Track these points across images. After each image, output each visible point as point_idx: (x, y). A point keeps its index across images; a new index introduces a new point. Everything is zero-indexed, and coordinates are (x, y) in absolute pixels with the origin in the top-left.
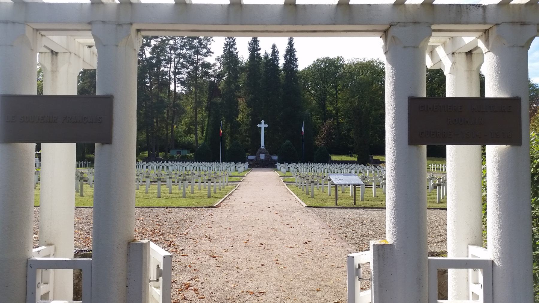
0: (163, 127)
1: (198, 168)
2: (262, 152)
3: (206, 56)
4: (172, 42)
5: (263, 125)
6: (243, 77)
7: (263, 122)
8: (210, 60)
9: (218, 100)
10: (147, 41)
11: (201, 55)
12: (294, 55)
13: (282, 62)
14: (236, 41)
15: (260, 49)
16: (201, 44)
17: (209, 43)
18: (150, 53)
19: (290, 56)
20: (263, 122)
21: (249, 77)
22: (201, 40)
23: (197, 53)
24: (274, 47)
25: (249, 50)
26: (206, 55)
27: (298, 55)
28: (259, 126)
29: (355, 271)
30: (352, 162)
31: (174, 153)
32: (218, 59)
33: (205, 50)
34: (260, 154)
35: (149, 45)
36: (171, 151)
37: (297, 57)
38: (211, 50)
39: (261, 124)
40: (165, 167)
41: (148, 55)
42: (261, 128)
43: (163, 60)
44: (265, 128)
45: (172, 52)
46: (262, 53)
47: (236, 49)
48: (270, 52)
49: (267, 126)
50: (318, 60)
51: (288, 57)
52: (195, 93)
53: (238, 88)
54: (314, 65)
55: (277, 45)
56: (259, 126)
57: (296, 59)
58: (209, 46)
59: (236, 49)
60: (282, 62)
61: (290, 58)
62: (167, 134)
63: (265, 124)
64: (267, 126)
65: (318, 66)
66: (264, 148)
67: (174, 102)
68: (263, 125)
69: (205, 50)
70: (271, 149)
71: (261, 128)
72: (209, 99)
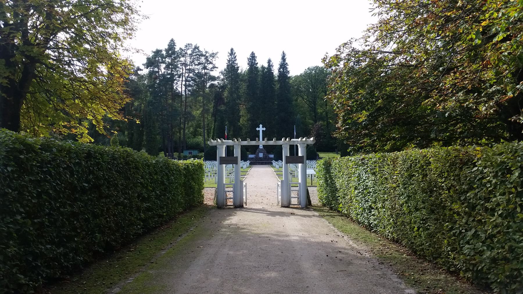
0: (177, 132)
3: (212, 71)
4: (182, 59)
6: (243, 87)
7: (261, 126)
8: (215, 73)
9: (223, 108)
10: (162, 60)
11: (208, 70)
13: (276, 72)
14: (237, 58)
15: (257, 63)
16: (208, 60)
17: (214, 59)
18: (164, 69)
19: (283, 69)
20: (261, 126)
21: (248, 87)
22: (207, 57)
23: (205, 68)
24: (269, 61)
25: (248, 64)
28: (257, 129)
29: (278, 185)
31: (186, 153)
32: (222, 72)
33: (210, 66)
35: (163, 62)
36: (184, 151)
37: (288, 70)
39: (259, 127)
41: (163, 70)
42: (259, 131)
43: (176, 75)
45: (184, 68)
46: (259, 66)
47: (237, 64)
48: (266, 65)
49: (264, 129)
50: (308, 69)
51: (281, 70)
52: (203, 102)
53: (239, 98)
54: (306, 73)
55: (272, 60)
56: (257, 129)
57: (288, 71)
58: (214, 62)
59: (237, 64)
60: (276, 72)
61: (283, 71)
62: (180, 137)
63: (263, 127)
64: (264, 129)
65: (309, 74)
66: (262, 148)
67: (185, 109)
69: (210, 66)
71: (259, 131)
72: (215, 107)
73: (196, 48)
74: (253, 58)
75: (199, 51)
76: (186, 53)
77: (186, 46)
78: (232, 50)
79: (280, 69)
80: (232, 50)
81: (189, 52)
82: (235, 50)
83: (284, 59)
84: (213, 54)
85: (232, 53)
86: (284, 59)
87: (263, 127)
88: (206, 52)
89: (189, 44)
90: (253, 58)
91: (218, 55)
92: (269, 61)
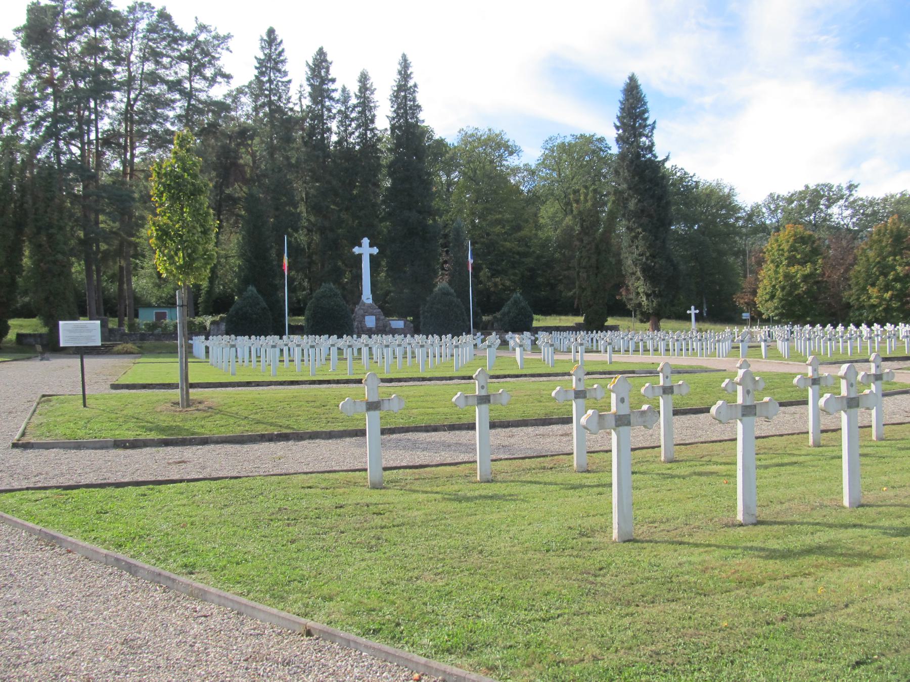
1: (286, 349)
2: (368, 311)
5: (366, 250)
7: (366, 241)
12: (414, 100)
20: (366, 241)
24: (364, 79)
26: (212, 81)
27: (421, 98)
28: (356, 250)
30: (577, 328)
34: (364, 316)
38: (226, 70)
40: (365, 351)
42: (360, 255)
44: (371, 255)
48: (354, 88)
49: (375, 251)
56: (356, 250)
57: (419, 107)
63: (371, 246)
64: (375, 251)
66: (370, 301)
68: (366, 250)
70: (386, 305)
71: (360, 255)
73: (164, 16)
74: (320, 67)
75: (175, 29)
76: (134, 29)
77: (132, 10)
78: (271, 32)
79: (397, 97)
80: (271, 32)
81: (142, 26)
82: (280, 35)
83: (405, 73)
84: (216, 37)
85: (271, 38)
86: (405, 73)
87: (371, 246)
88: (203, 28)
89: (141, 5)
90: (320, 67)
91: (231, 43)
92: (364, 79)
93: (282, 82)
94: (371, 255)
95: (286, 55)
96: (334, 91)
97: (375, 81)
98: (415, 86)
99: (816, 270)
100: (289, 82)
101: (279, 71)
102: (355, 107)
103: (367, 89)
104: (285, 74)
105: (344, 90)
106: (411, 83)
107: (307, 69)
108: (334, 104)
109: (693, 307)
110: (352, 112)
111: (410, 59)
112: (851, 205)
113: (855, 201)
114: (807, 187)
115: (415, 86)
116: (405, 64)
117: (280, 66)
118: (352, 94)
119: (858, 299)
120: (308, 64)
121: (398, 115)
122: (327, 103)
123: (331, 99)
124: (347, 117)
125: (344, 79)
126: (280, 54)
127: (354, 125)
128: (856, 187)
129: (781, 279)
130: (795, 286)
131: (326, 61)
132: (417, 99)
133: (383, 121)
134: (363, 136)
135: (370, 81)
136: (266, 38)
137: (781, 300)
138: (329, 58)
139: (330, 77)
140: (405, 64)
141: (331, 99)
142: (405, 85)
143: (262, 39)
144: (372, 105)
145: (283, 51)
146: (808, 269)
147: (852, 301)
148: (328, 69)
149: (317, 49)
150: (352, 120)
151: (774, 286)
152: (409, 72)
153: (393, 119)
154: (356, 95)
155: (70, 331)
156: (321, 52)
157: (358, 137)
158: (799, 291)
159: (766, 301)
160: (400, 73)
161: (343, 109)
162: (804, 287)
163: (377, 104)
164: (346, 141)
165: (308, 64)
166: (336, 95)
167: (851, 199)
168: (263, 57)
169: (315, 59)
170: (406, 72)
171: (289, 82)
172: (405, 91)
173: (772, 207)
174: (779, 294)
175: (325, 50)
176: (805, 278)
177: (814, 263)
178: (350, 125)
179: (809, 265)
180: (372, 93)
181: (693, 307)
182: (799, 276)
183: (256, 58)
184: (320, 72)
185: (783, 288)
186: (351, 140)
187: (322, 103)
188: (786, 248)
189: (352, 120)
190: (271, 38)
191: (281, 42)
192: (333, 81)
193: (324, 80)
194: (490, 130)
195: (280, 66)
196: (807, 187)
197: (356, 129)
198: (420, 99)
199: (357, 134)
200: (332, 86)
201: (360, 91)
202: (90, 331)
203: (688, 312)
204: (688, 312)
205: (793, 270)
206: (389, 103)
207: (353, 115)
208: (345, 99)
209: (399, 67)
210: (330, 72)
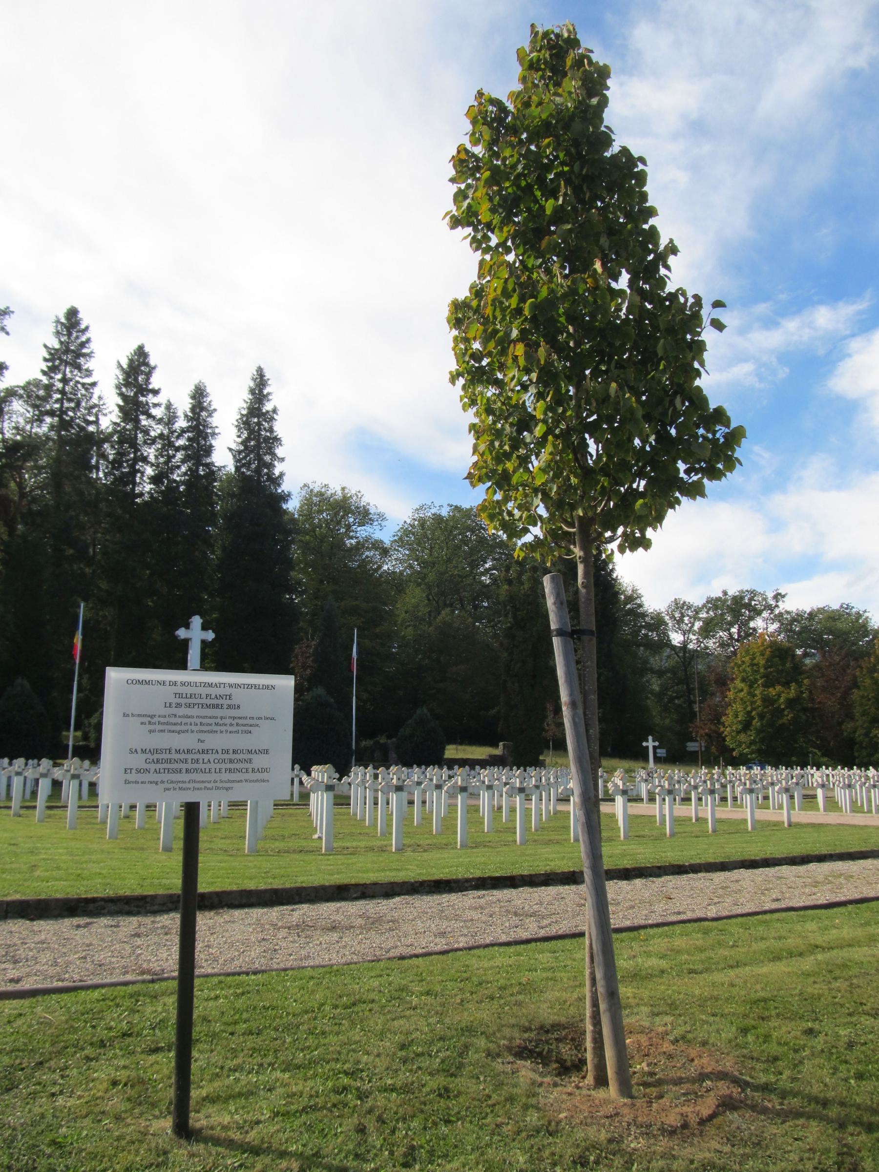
7: (196, 621)
12: (271, 430)
20: (196, 621)
24: (199, 395)
28: (182, 633)
42: (186, 642)
44: (203, 642)
48: (183, 405)
49: (210, 636)
56: (182, 633)
57: (277, 439)
63: (204, 628)
64: (210, 636)
71: (186, 642)
74: (137, 372)
78: (72, 313)
80: (72, 313)
82: (85, 318)
85: (71, 322)
87: (204, 628)
90: (137, 372)
92: (199, 395)
93: (83, 385)
94: (203, 642)
95: (93, 346)
96: (156, 405)
97: (214, 399)
98: (275, 411)
99: (802, 693)
100: (94, 384)
101: (79, 367)
102: (183, 431)
103: (203, 409)
104: (89, 373)
105: (169, 406)
106: (268, 407)
107: (118, 372)
108: (153, 424)
109: (650, 738)
110: (178, 437)
111: (268, 375)
112: (779, 617)
113: (781, 614)
114: (725, 593)
115: (275, 411)
116: (260, 381)
117: (82, 361)
118: (180, 413)
119: (867, 734)
120: (120, 366)
121: (246, 448)
122: (144, 423)
123: (150, 416)
124: (171, 444)
125: (171, 390)
126: (83, 345)
127: (179, 456)
128: (783, 596)
129: (759, 703)
130: (778, 713)
131: (147, 364)
132: (275, 428)
133: (223, 456)
134: (193, 472)
135: (209, 399)
136: (63, 320)
137: (759, 731)
138: (152, 361)
139: (151, 387)
140: (260, 381)
141: (150, 416)
142: (259, 409)
143: (58, 321)
144: (209, 431)
145: (88, 340)
146: (792, 692)
147: (859, 735)
148: (149, 375)
149: (136, 347)
150: (178, 449)
151: (749, 713)
152: (265, 392)
153: (240, 452)
154: (186, 416)
155: (149, 719)
156: (141, 354)
157: (185, 474)
158: (784, 720)
159: (738, 732)
160: (252, 391)
161: (166, 432)
162: (789, 716)
163: (217, 431)
164: (167, 478)
165: (120, 366)
166: (158, 412)
167: (777, 611)
168: (57, 346)
169: (131, 361)
170: (261, 391)
171: (94, 384)
172: (258, 417)
173: (677, 615)
174: (756, 723)
175: (146, 349)
176: (791, 703)
177: (799, 684)
178: (174, 456)
179: (793, 686)
180: (210, 415)
181: (650, 738)
182: (782, 700)
183: (45, 346)
184: (136, 379)
185: (761, 716)
186: (175, 477)
187: (137, 421)
188: (762, 662)
189: (178, 449)
190: (71, 322)
191: (87, 328)
192: (156, 392)
193: (144, 390)
194: (343, 489)
195: (82, 361)
196: (725, 593)
197: (183, 461)
198: (280, 428)
199: (183, 469)
200: (151, 399)
201: (193, 410)
202: (246, 725)
203: (644, 744)
204: (644, 744)
205: (772, 692)
206: (235, 431)
207: (181, 442)
208: (170, 419)
209: (252, 384)
210: (152, 380)
